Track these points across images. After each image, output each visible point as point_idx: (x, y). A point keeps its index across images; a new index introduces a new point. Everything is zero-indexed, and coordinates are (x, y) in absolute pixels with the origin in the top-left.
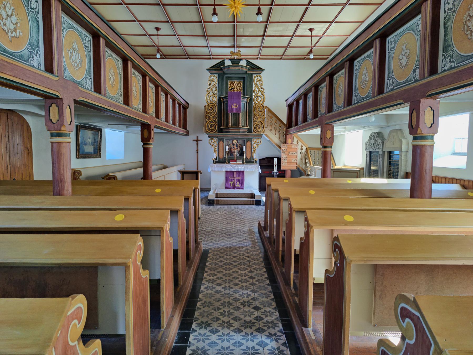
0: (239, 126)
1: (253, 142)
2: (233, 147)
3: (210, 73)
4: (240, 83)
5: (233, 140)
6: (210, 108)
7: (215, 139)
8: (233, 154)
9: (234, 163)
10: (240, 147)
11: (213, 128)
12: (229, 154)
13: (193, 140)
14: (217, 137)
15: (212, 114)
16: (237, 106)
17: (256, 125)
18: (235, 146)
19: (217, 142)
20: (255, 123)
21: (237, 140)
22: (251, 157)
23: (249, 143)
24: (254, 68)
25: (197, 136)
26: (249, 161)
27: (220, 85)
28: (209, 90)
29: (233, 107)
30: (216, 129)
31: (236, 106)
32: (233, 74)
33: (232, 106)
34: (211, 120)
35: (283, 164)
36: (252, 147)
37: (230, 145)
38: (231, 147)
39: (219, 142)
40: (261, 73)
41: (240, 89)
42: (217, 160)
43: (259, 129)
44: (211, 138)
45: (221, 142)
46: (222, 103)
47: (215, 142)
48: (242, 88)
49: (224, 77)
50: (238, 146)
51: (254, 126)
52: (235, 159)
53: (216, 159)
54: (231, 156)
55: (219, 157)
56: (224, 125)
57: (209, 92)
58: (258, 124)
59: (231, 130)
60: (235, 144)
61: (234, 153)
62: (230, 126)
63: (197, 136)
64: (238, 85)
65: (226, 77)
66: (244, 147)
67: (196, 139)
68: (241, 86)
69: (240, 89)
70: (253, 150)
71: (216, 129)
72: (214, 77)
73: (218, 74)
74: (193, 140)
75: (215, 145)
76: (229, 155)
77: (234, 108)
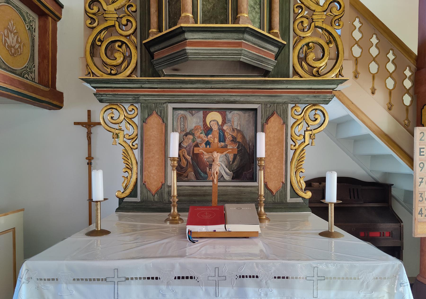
0: (236, 20)
1: (291, 121)
2: (208, 143)
5: (206, 111)
7: (127, 106)
8: (206, 173)
9: (211, 228)
10: (234, 140)
12: (190, 169)
13: (76, 124)
14: (136, 99)
17: (307, 44)
18: (214, 138)
19: (136, 120)
20: (302, 34)
21: (222, 111)
22: (284, 185)
23: (275, 122)
25: (89, 112)
26: (277, 199)
30: (133, 61)
34: (110, 23)
35: (421, 213)
36: (290, 142)
37: (191, 133)
38: (199, 140)
39: (144, 121)
42: (138, 199)
43: (317, 64)
44: (111, 102)
45: (154, 120)
47: (129, 120)
50: (229, 138)
51: (299, 47)
52: (215, 199)
53: (133, 194)
54: (198, 178)
55: (144, 184)
58: (315, 39)
59: (193, 44)
60: (215, 128)
61: (211, 166)
62: (187, 22)
63: (89, 112)
66: (261, 138)
67: (85, 119)
70: (291, 153)
71: (133, 61)
74: (76, 124)
75: (131, 131)
76: (192, 175)
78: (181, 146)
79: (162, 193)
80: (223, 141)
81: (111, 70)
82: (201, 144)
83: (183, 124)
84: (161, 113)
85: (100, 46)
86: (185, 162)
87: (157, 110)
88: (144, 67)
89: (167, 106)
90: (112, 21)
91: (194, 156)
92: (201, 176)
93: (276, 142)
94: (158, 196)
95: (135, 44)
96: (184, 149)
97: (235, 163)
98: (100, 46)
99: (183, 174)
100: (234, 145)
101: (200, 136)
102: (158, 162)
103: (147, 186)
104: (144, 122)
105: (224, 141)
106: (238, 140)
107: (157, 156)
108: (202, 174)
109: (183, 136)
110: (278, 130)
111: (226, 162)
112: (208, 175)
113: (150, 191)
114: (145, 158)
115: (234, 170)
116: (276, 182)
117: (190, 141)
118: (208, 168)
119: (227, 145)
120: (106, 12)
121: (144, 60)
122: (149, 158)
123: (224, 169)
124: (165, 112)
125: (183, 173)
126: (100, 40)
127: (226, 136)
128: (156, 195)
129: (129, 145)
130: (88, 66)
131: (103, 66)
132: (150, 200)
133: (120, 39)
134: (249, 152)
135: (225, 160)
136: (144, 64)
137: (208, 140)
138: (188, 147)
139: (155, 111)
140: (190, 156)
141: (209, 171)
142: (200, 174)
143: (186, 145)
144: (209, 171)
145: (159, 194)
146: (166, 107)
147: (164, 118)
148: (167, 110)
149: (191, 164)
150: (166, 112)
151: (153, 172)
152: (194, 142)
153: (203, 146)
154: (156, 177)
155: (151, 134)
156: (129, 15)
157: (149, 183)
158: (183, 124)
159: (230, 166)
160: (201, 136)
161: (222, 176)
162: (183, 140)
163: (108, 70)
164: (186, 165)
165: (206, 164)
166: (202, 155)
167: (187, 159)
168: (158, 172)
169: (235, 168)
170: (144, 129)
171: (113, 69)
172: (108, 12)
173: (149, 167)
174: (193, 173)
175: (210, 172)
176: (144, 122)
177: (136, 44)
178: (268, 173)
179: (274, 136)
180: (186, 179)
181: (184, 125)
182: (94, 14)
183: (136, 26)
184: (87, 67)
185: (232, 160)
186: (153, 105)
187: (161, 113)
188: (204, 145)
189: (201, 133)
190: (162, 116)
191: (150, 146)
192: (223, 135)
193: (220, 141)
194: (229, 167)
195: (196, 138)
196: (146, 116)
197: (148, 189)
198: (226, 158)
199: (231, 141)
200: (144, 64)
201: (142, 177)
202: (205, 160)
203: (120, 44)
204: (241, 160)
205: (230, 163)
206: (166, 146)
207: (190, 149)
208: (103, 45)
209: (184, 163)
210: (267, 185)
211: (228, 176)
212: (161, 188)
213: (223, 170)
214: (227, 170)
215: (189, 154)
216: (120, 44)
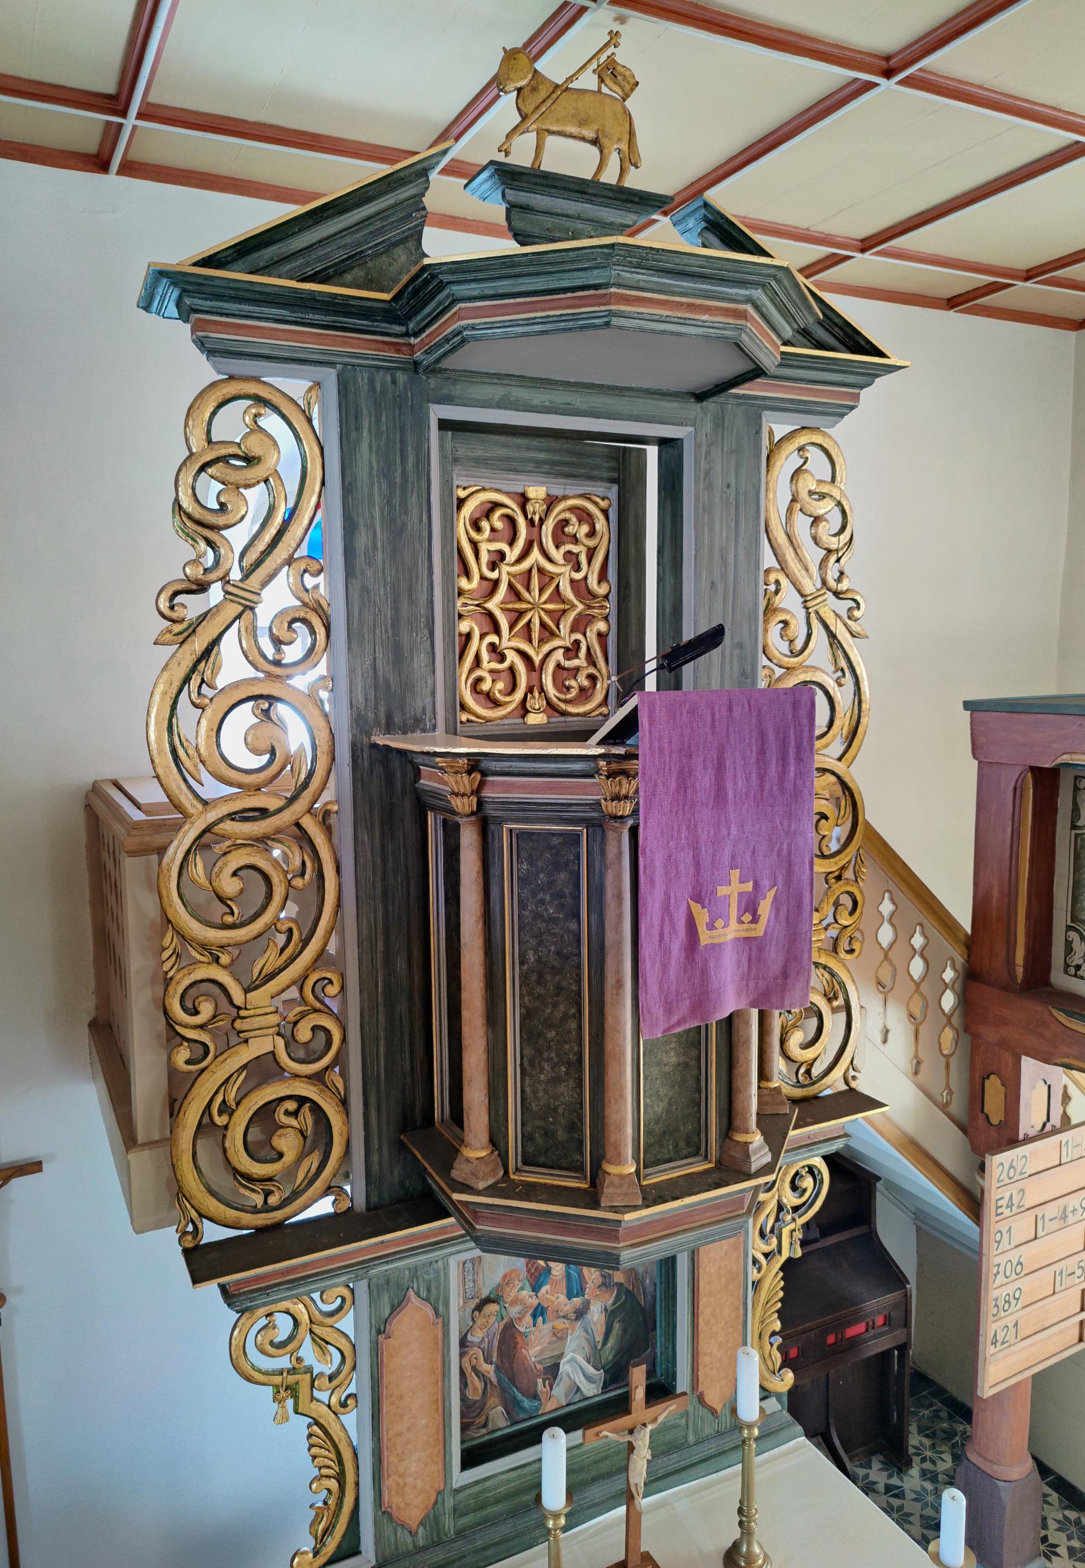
3: (211, 350)
4: (584, 516)
6: (230, 886)
11: (288, 1143)
15: (270, 959)
16: (765, 908)
24: (833, 349)
27: (362, 540)
28: (192, 606)
29: (705, 937)
31: (750, 906)
32: (539, 397)
33: (702, 917)
34: (259, 1047)
38: (514, 1311)
40: (840, 412)
41: (580, 587)
46: (469, 838)
48: (603, 577)
49: (422, 423)
56: (496, 1140)
57: (198, 644)
64: (560, 535)
65: (445, 425)
68: (591, 553)
69: (580, 587)
72: (271, 422)
73: (330, 377)
77: (716, 948)
78: (468, 1344)
79: (436, 1518)
80: (578, 1293)
81: (267, 1194)
82: (520, 1319)
83: (470, 1278)
84: (429, 1290)
85: (226, 1127)
86: (479, 1385)
87: (418, 1286)
88: (375, 1168)
89: (446, 1266)
90: (265, 1038)
91: (502, 1361)
92: (522, 1408)
93: (724, 1280)
94: (428, 1528)
95: (340, 1093)
96: (476, 1348)
97: (609, 1345)
98: (226, 1127)
99: (474, 1422)
100: (607, 1295)
101: (517, 1299)
102: (425, 1437)
103: (395, 1514)
104: (379, 1332)
105: (581, 1292)
106: (615, 1281)
107: (423, 1422)
108: (526, 1403)
109: (473, 1312)
110: (727, 1251)
111: (587, 1350)
112: (540, 1400)
113: (403, 1526)
114: (389, 1440)
115: (608, 1363)
116: (725, 1381)
117: (493, 1320)
118: (540, 1381)
119: (588, 1302)
120: (243, 1013)
121: (377, 1147)
122: (399, 1434)
123: (581, 1369)
124: (440, 1284)
125: (474, 1418)
126: (224, 1108)
127: (587, 1278)
128: (421, 1531)
129: (329, 1406)
130: (186, 1199)
131: (237, 1185)
132: (405, 1550)
133: (293, 1091)
134: (643, 1304)
135: (585, 1344)
136: (375, 1158)
137: (539, 1304)
138: (486, 1339)
139: (412, 1288)
140: (491, 1363)
141: (544, 1386)
142: (518, 1403)
143: (480, 1335)
144: (544, 1386)
145: (430, 1526)
146: (444, 1268)
147: (437, 1302)
148: (447, 1275)
149: (494, 1380)
150: (445, 1281)
151: (413, 1469)
152: (503, 1319)
153: (527, 1323)
154: (423, 1480)
155: (404, 1362)
156: (316, 1011)
157: (402, 1505)
158: (470, 1278)
159: (598, 1355)
160: (520, 1297)
161: (578, 1389)
162: (471, 1324)
163: (254, 1196)
164: (480, 1391)
165: (535, 1371)
166: (523, 1350)
167: (483, 1376)
168: (426, 1465)
169: (610, 1358)
170: (382, 1353)
171: (272, 1188)
172: (251, 1013)
173: (400, 1461)
174: (501, 1408)
175: (545, 1390)
176: (379, 1332)
177: (342, 1093)
178: (706, 1366)
179: (720, 1268)
180: (484, 1431)
181: (474, 1281)
182: (201, 1027)
183: (344, 1040)
184: (181, 1202)
185: (602, 1337)
186: (407, 1272)
187: (429, 1290)
188: (528, 1318)
189: (522, 1289)
190: (432, 1299)
191: (401, 1398)
192: (579, 1276)
193: (570, 1296)
194: (595, 1358)
195: (507, 1305)
196: (387, 1312)
197: (396, 1522)
198: (588, 1337)
199: (599, 1287)
200: (375, 1158)
201: (377, 1493)
202: (533, 1359)
203: (291, 1106)
204: (624, 1331)
205: (596, 1347)
206: (446, 1380)
207: (490, 1343)
208: (238, 1123)
209: (475, 1389)
210: (703, 1399)
211: (593, 1385)
212: (436, 1503)
213: (580, 1372)
214: (590, 1370)
215: (488, 1360)
216: (291, 1106)
